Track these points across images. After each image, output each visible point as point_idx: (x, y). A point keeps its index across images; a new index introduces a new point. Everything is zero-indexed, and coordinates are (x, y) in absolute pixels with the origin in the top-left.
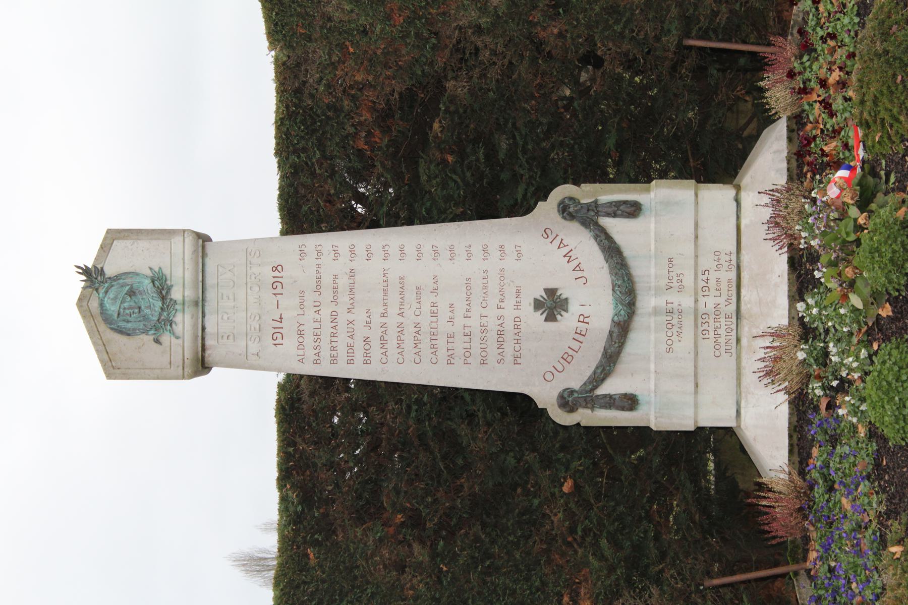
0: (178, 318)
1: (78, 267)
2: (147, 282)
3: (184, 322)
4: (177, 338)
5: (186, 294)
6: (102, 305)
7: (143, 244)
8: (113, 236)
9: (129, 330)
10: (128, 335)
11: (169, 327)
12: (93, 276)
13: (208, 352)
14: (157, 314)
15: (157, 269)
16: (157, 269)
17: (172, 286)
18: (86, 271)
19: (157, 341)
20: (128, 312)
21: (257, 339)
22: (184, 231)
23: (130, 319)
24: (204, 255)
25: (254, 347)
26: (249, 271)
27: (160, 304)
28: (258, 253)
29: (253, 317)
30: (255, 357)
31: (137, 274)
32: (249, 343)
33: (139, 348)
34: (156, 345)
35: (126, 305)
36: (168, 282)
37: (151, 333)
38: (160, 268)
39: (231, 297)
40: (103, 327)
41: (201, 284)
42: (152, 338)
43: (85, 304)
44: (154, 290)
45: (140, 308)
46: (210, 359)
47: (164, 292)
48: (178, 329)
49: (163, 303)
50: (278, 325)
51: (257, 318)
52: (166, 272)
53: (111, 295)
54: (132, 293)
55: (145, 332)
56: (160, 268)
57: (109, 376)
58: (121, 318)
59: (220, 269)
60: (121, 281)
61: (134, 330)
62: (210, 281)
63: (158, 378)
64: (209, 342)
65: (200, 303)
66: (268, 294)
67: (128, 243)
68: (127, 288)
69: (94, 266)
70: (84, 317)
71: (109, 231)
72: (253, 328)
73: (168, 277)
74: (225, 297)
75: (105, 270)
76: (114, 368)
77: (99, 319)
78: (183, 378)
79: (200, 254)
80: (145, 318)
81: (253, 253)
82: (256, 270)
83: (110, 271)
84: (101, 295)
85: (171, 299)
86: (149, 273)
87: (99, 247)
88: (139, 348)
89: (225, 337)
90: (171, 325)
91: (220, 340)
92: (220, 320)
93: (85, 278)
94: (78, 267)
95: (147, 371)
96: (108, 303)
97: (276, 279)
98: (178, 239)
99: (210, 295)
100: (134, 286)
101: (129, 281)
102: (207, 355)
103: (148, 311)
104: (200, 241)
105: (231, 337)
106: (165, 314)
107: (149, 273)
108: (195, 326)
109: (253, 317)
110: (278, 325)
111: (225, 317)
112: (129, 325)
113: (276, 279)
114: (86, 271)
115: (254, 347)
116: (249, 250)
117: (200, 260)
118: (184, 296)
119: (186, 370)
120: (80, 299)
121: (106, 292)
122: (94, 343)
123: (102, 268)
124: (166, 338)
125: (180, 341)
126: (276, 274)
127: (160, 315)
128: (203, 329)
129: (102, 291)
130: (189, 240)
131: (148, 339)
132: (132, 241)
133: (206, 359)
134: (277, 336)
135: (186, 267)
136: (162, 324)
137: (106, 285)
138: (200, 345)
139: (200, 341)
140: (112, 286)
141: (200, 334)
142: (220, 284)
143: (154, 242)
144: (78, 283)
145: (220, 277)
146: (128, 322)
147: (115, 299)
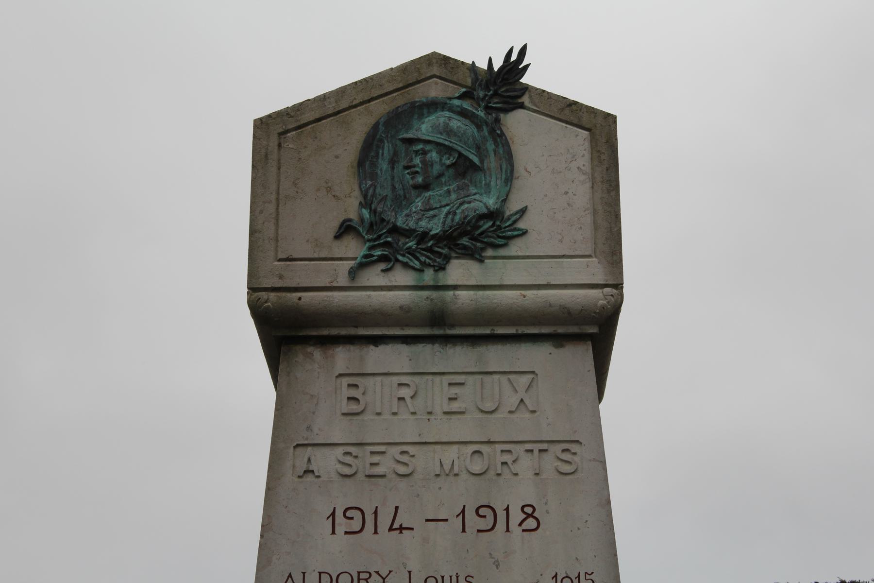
0: (402, 277)
1: (523, 51)
2: (491, 202)
3: (393, 289)
4: (353, 273)
5: (463, 294)
6: (434, 105)
7: (582, 194)
8: (598, 130)
9: (374, 165)
10: (361, 163)
11: (378, 253)
12: (503, 85)
13: (317, 353)
14: (412, 224)
15: (521, 225)
16: (521, 225)
17: (481, 261)
18: (514, 67)
19: (345, 229)
20: (417, 161)
21: (347, 471)
22: (618, 286)
23: (399, 167)
24: (559, 340)
25: (327, 462)
26: (519, 449)
27: (436, 228)
28: (566, 468)
29: (405, 458)
30: (302, 466)
31: (509, 178)
32: (340, 450)
33: (329, 189)
34: (336, 224)
35: (434, 155)
36: (490, 252)
37: (366, 213)
38: (524, 233)
39: (455, 406)
40: (380, 109)
41: (487, 331)
42: (353, 215)
43: (435, 70)
44: (472, 214)
45: (425, 187)
46: (300, 358)
47: (465, 241)
48: (374, 276)
49: (438, 238)
50: (385, 521)
51: (402, 470)
52: (516, 248)
53: (457, 123)
54: (464, 169)
55: (366, 203)
56: (524, 233)
57: (262, 125)
58: (402, 148)
59: (525, 379)
60: (490, 146)
61: (374, 176)
62: (496, 357)
63: (253, 232)
64: (343, 358)
65: (438, 327)
66: (463, 493)
67: (583, 160)
68: (476, 160)
69: (526, 88)
70: (404, 69)
71: (610, 120)
72: (376, 459)
73: (502, 252)
74: (455, 390)
75: (520, 113)
76: (281, 136)
77: (399, 100)
78: (252, 289)
79: (561, 330)
80: (401, 201)
81: (566, 456)
82: (526, 465)
83: (518, 124)
84: (457, 102)
85: (447, 259)
86: (514, 206)
87: (572, 97)
88: (329, 189)
89: (353, 393)
90: (383, 259)
91: (345, 381)
92: (396, 380)
93: (496, 66)
94: (523, 51)
95: (271, 208)
96: (441, 117)
97: (501, 515)
98: (595, 272)
99: (460, 358)
100: (480, 176)
101: (492, 162)
102: (310, 349)
103: (419, 204)
104: (593, 330)
105: (354, 407)
106: (412, 244)
107: (514, 206)
108: (380, 317)
109: (405, 458)
110: (385, 521)
111: (405, 392)
112: (384, 165)
113: (501, 515)
114: (514, 67)
115: (327, 462)
116: (574, 448)
117: (545, 330)
118: (455, 287)
119: (272, 295)
120: (446, 60)
121: (463, 113)
122: (342, 92)
123: (522, 106)
124: (353, 249)
125: (343, 281)
126: (516, 516)
127: (408, 233)
128: (376, 341)
129: (466, 105)
130: (597, 297)
131: (351, 208)
132: (587, 168)
133: (298, 347)
134: (356, 520)
135: (528, 293)
136: (384, 240)
137: (482, 114)
138: (334, 332)
139: (344, 332)
140: (479, 127)
141: (362, 332)
142: (488, 379)
143: (588, 219)
144: (482, 51)
145: (504, 379)
146: (393, 162)
147: (448, 131)
